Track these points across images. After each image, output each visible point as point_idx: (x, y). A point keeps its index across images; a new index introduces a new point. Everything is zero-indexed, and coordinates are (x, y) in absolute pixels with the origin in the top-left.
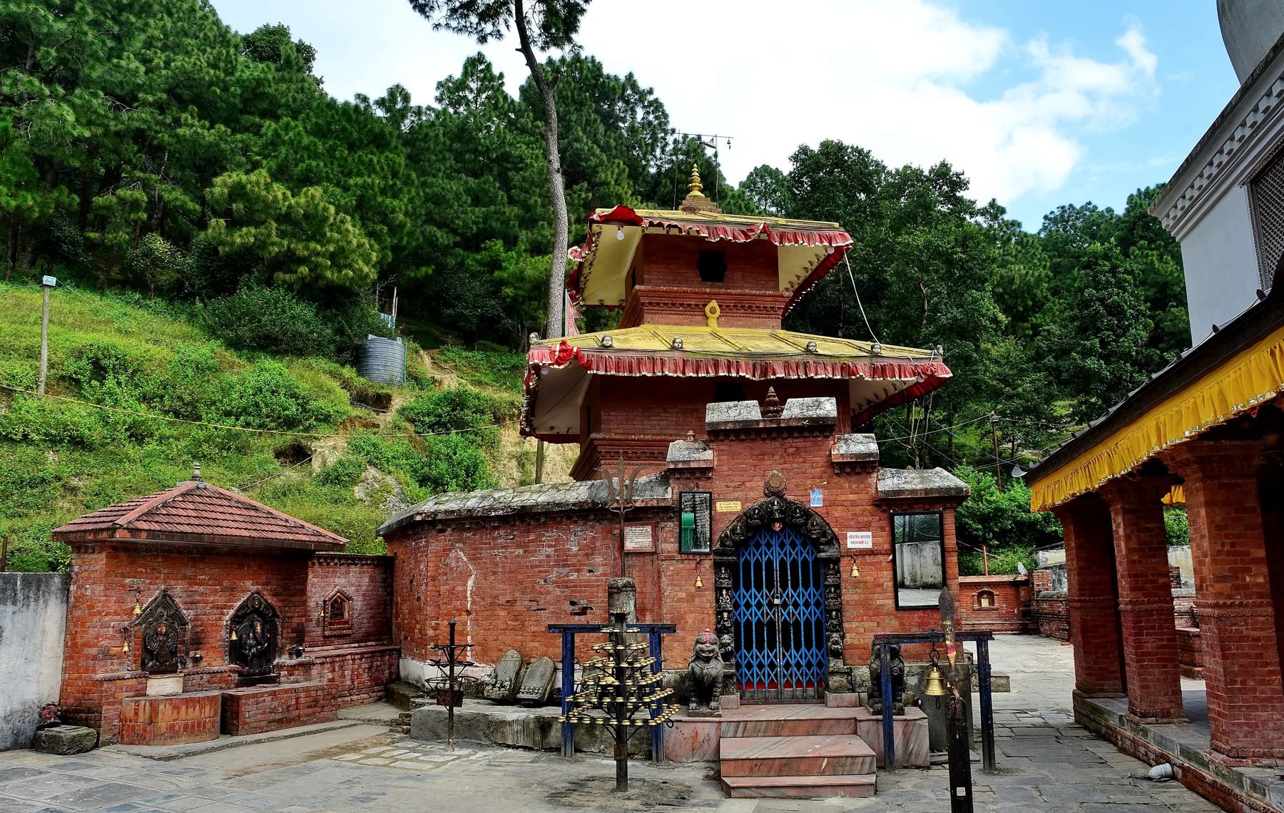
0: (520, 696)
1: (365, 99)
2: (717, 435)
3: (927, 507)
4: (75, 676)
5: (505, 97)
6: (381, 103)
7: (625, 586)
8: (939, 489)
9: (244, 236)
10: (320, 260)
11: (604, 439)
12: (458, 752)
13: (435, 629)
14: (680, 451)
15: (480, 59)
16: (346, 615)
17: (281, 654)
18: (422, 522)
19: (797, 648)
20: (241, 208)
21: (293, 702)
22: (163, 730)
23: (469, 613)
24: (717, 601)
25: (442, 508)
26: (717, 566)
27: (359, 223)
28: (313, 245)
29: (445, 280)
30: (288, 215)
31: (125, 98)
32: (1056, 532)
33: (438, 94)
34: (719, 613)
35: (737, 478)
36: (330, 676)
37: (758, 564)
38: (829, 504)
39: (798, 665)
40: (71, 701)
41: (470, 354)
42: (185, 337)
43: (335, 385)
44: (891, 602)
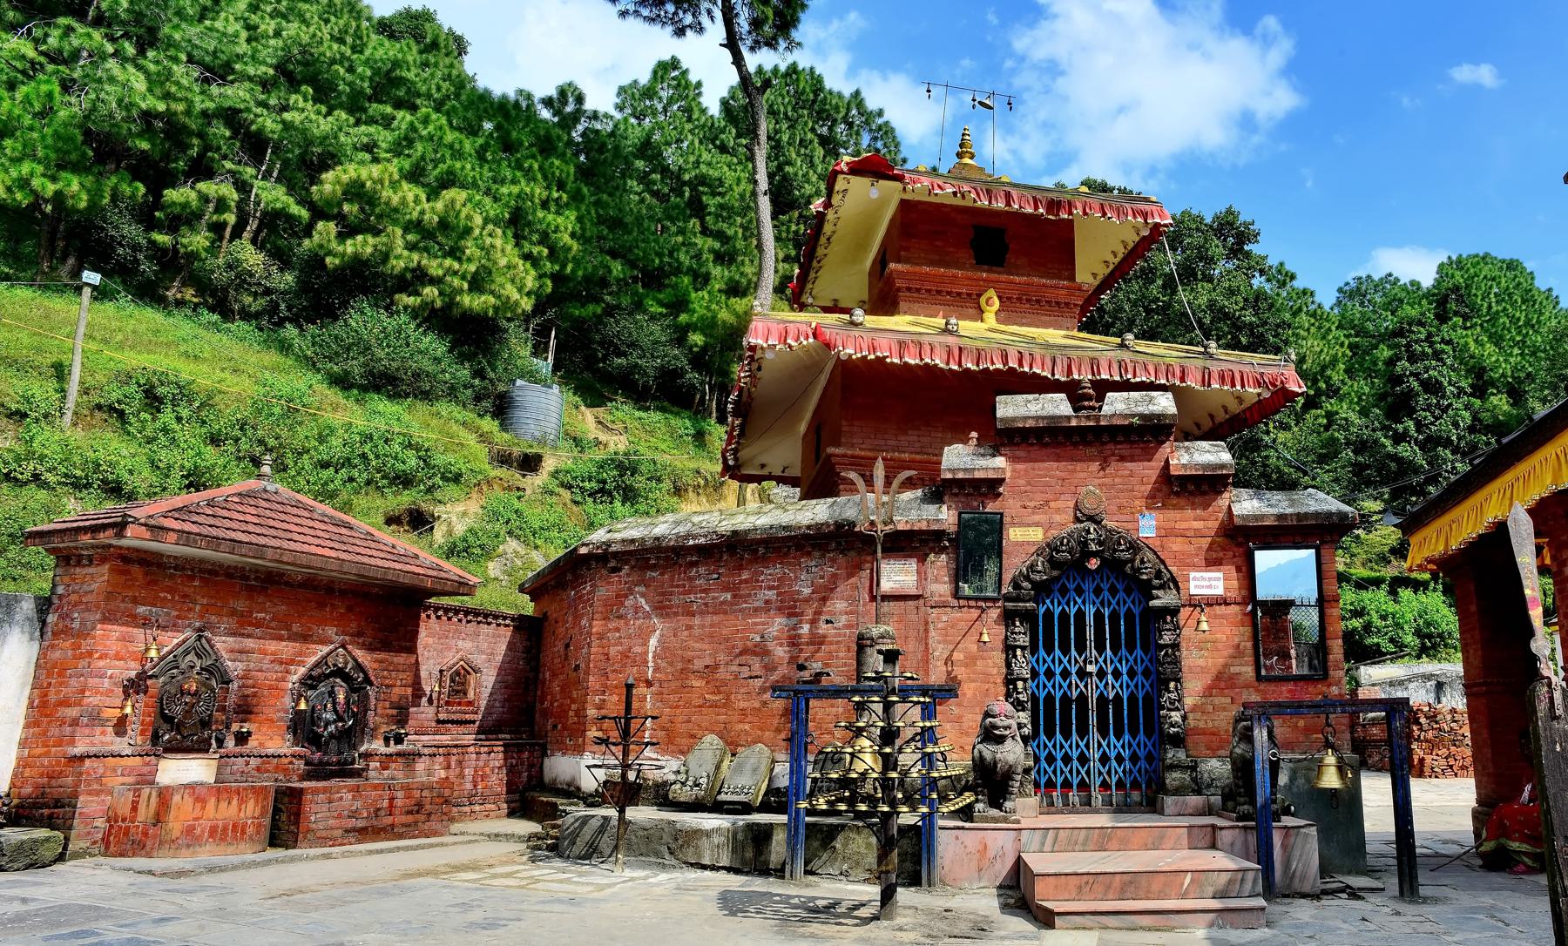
4: (39, 751)
7: (883, 637)
9: (362, 245)
11: (844, 456)
12: (628, 873)
13: (599, 708)
14: (959, 458)
16: (471, 695)
18: (590, 556)
21: (386, 804)
22: (176, 834)
23: (649, 684)
24: (1008, 665)
25: (618, 536)
26: (1008, 617)
28: (448, 262)
29: (617, 322)
30: (420, 222)
35: (1039, 496)
36: (443, 774)
40: (28, 790)
42: (274, 369)
43: (471, 440)
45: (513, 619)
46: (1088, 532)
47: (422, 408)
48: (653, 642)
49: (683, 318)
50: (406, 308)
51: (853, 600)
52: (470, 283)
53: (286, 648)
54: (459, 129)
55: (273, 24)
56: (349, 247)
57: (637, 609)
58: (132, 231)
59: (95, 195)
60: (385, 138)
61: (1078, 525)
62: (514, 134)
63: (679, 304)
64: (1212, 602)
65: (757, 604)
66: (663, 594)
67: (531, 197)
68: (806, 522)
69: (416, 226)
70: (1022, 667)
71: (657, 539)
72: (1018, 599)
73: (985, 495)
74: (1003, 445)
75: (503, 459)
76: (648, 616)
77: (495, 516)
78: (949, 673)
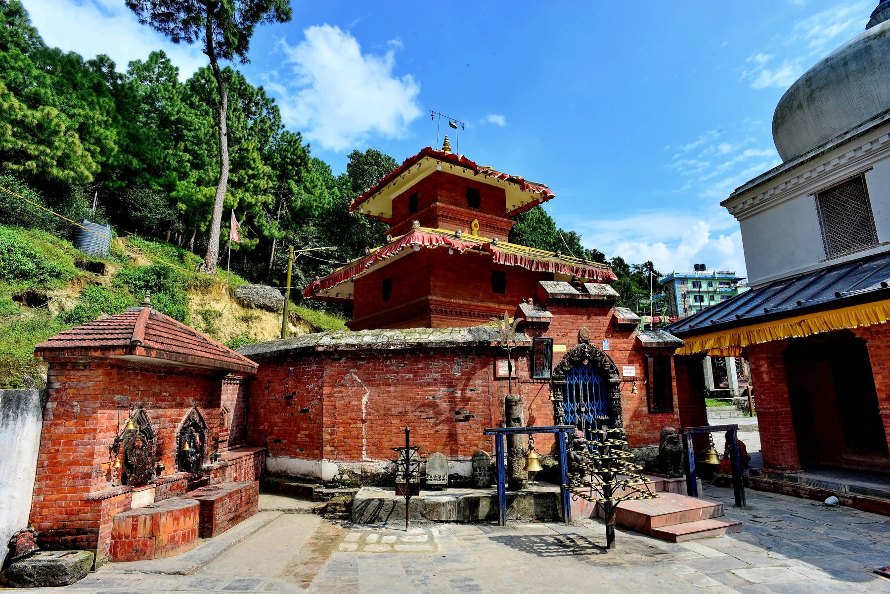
0: (429, 482)
2: (545, 301)
6: (92, 63)
10: (48, 160)
11: (436, 301)
13: (331, 434)
18: (325, 352)
23: (363, 421)
24: (556, 410)
26: (554, 388)
29: (134, 192)
35: (563, 331)
38: (613, 349)
41: (150, 243)
48: (365, 399)
49: (174, 194)
50: (12, 170)
51: (486, 380)
52: (58, 161)
57: (353, 381)
63: (170, 187)
64: (632, 380)
65: (429, 380)
66: (369, 374)
67: (93, 119)
69: (21, 123)
73: (541, 329)
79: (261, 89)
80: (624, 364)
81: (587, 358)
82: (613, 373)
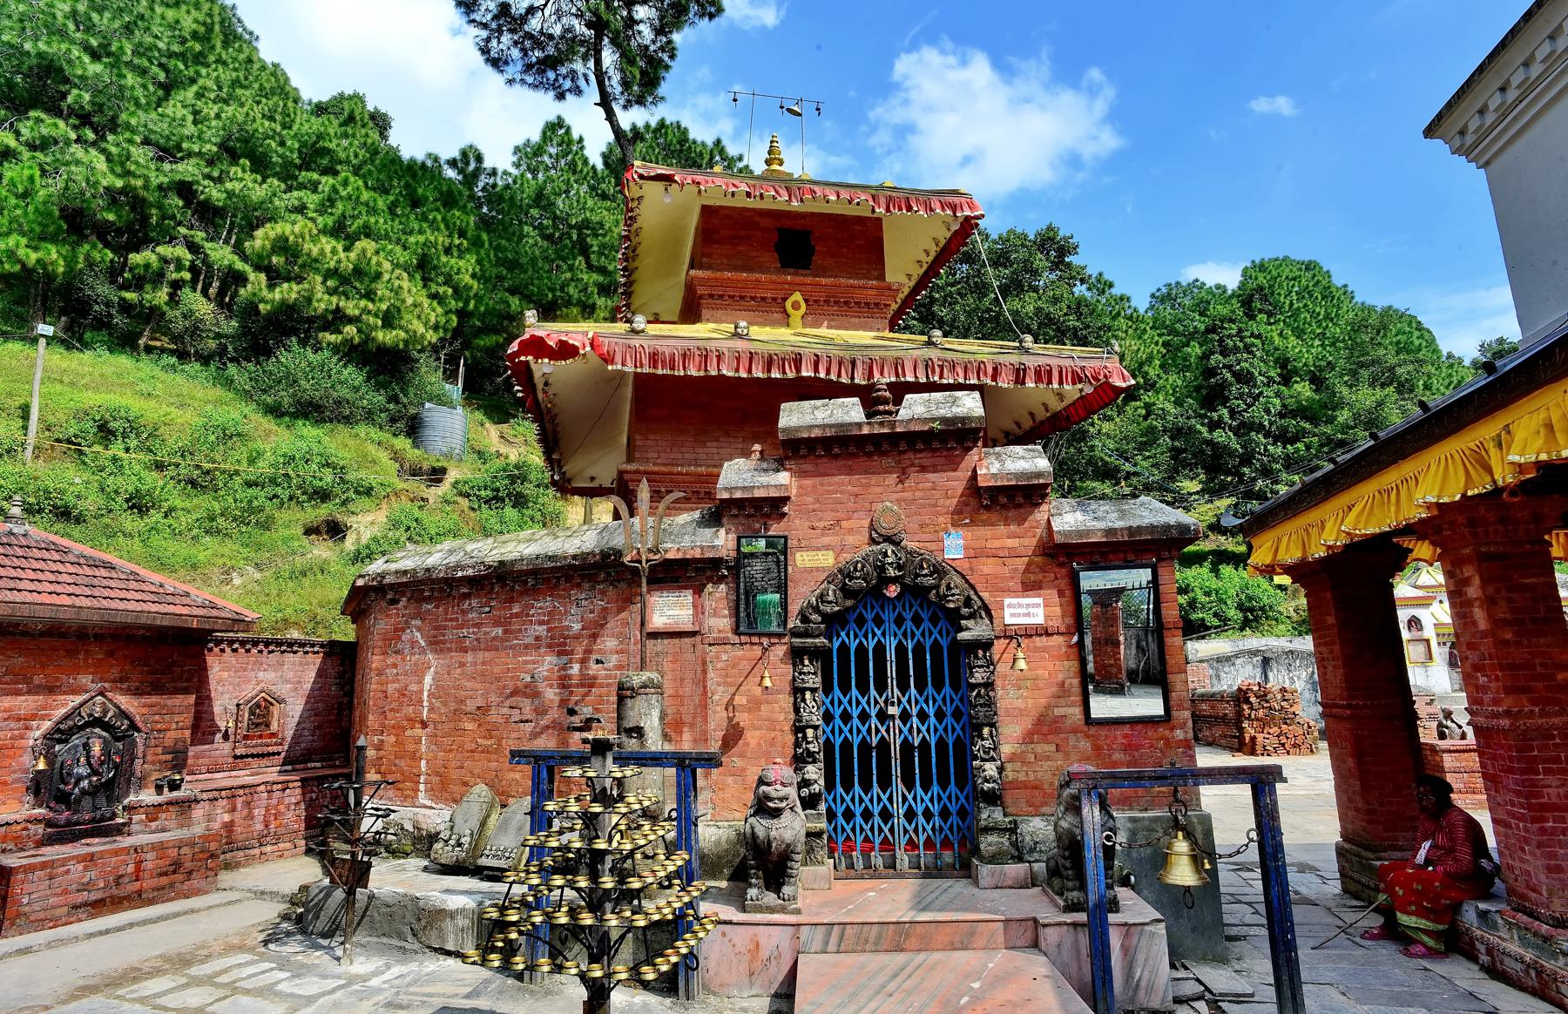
0: (483, 862)
1: (436, 159)
2: (800, 451)
3: (1131, 557)
5: (586, 162)
6: (453, 163)
7: (645, 686)
8: (1152, 528)
9: (288, 291)
13: (379, 748)
14: (740, 474)
15: (560, 123)
16: (274, 727)
17: (142, 783)
19: (926, 788)
20: (286, 263)
21: (131, 869)
24: (797, 710)
25: (393, 567)
26: (796, 655)
27: (420, 284)
28: (363, 303)
30: (336, 270)
31: (168, 151)
32: (1203, 620)
33: (515, 159)
34: (799, 729)
36: (227, 818)
37: (861, 650)
38: (974, 554)
39: (928, 815)
42: (218, 402)
43: (383, 456)
44: (1076, 712)
45: (322, 646)
46: (886, 555)
47: (343, 431)
48: (428, 680)
50: (329, 344)
51: (623, 638)
53: (25, 703)
54: (374, 189)
55: (216, 108)
56: (277, 295)
57: (413, 643)
58: (104, 290)
59: (70, 262)
60: (312, 200)
61: (874, 548)
62: (420, 191)
66: (437, 628)
67: (435, 245)
68: (572, 551)
70: (812, 712)
71: (428, 570)
72: (806, 634)
73: (768, 516)
74: (787, 458)
75: (415, 472)
76: (423, 652)
77: (395, 525)
78: (730, 719)
79: (718, 142)
80: (1012, 592)
81: (894, 580)
82: (971, 616)
